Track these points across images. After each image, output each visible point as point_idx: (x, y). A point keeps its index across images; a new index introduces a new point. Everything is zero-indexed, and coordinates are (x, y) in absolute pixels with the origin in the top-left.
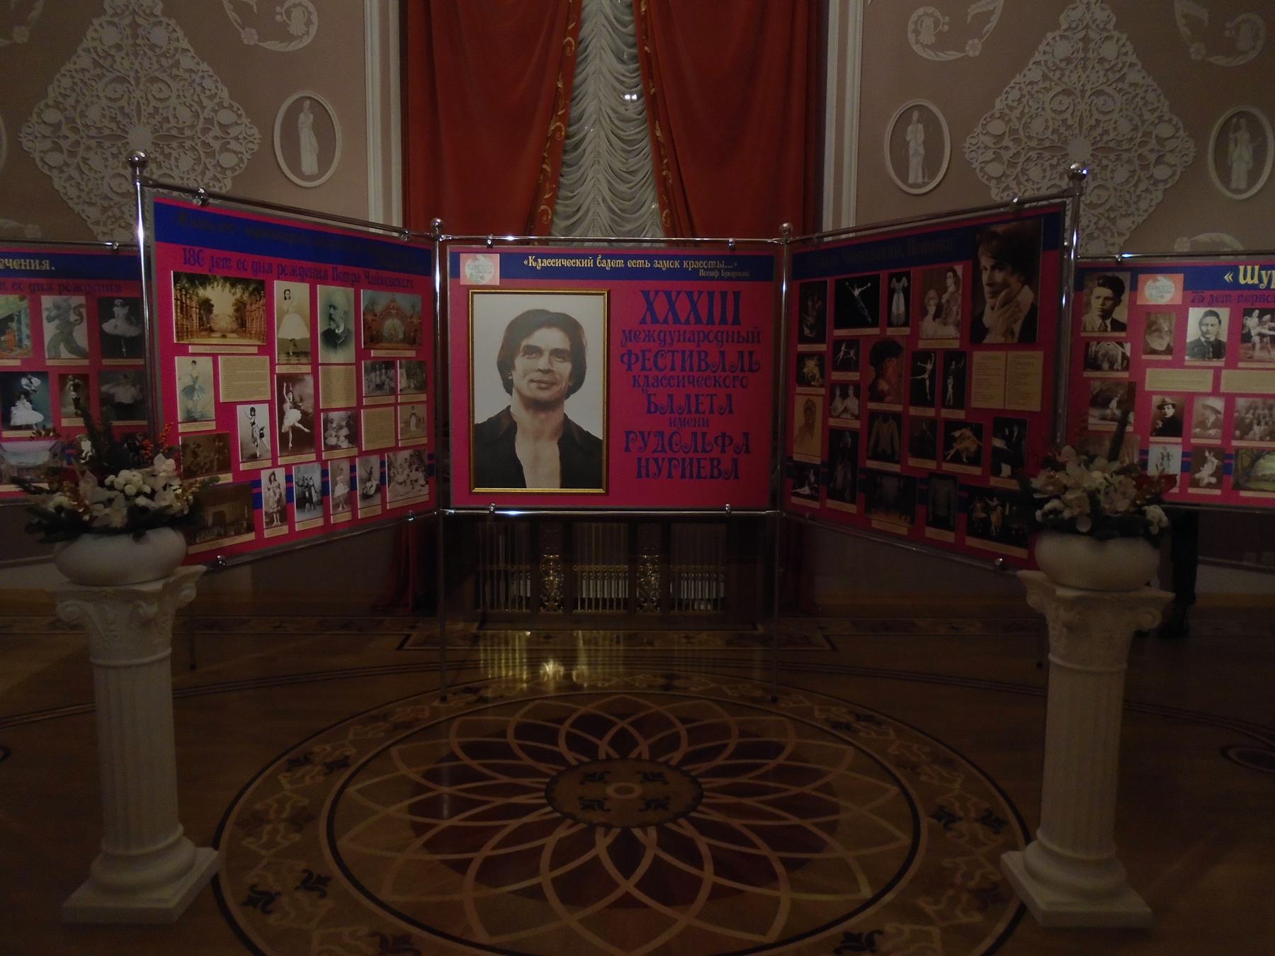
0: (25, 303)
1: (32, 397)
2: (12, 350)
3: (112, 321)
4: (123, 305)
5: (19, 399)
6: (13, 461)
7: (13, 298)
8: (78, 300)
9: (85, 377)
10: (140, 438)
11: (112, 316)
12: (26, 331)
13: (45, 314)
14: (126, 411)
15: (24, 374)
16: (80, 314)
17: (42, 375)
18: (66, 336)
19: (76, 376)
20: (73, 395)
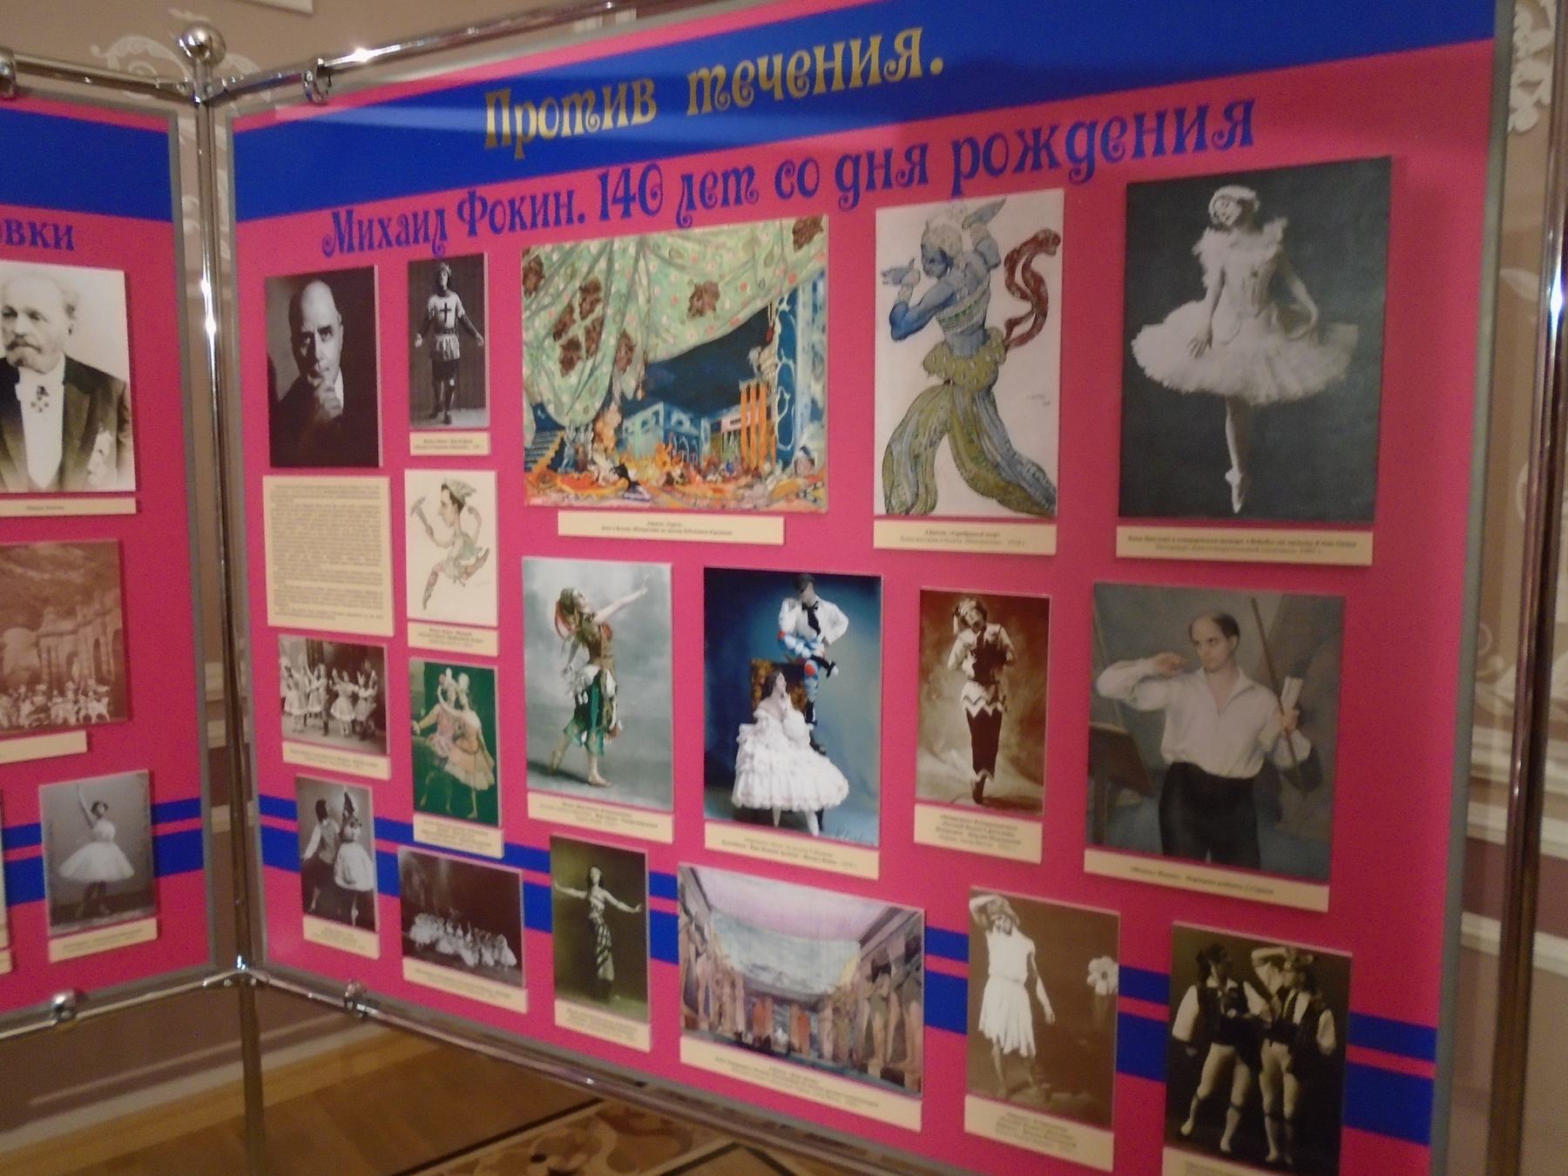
0: (817, 252)
1: (816, 687)
2: (757, 475)
3: (1187, 318)
4: (1252, 220)
5: (767, 691)
6: (734, 954)
7: (773, 232)
8: (1037, 210)
9: (1026, 614)
10: (1274, 980)
11: (1188, 285)
12: (810, 386)
13: (886, 297)
14: (1211, 817)
15: (789, 583)
16: (1034, 292)
17: (857, 590)
18: (966, 409)
19: (993, 608)
20: (972, 696)
